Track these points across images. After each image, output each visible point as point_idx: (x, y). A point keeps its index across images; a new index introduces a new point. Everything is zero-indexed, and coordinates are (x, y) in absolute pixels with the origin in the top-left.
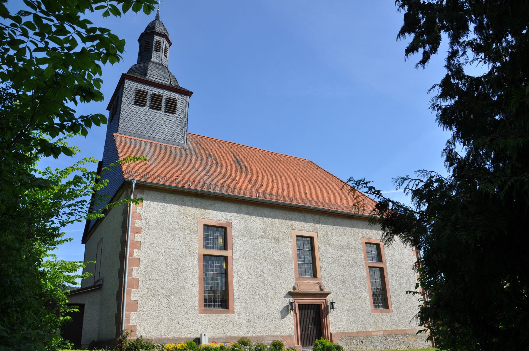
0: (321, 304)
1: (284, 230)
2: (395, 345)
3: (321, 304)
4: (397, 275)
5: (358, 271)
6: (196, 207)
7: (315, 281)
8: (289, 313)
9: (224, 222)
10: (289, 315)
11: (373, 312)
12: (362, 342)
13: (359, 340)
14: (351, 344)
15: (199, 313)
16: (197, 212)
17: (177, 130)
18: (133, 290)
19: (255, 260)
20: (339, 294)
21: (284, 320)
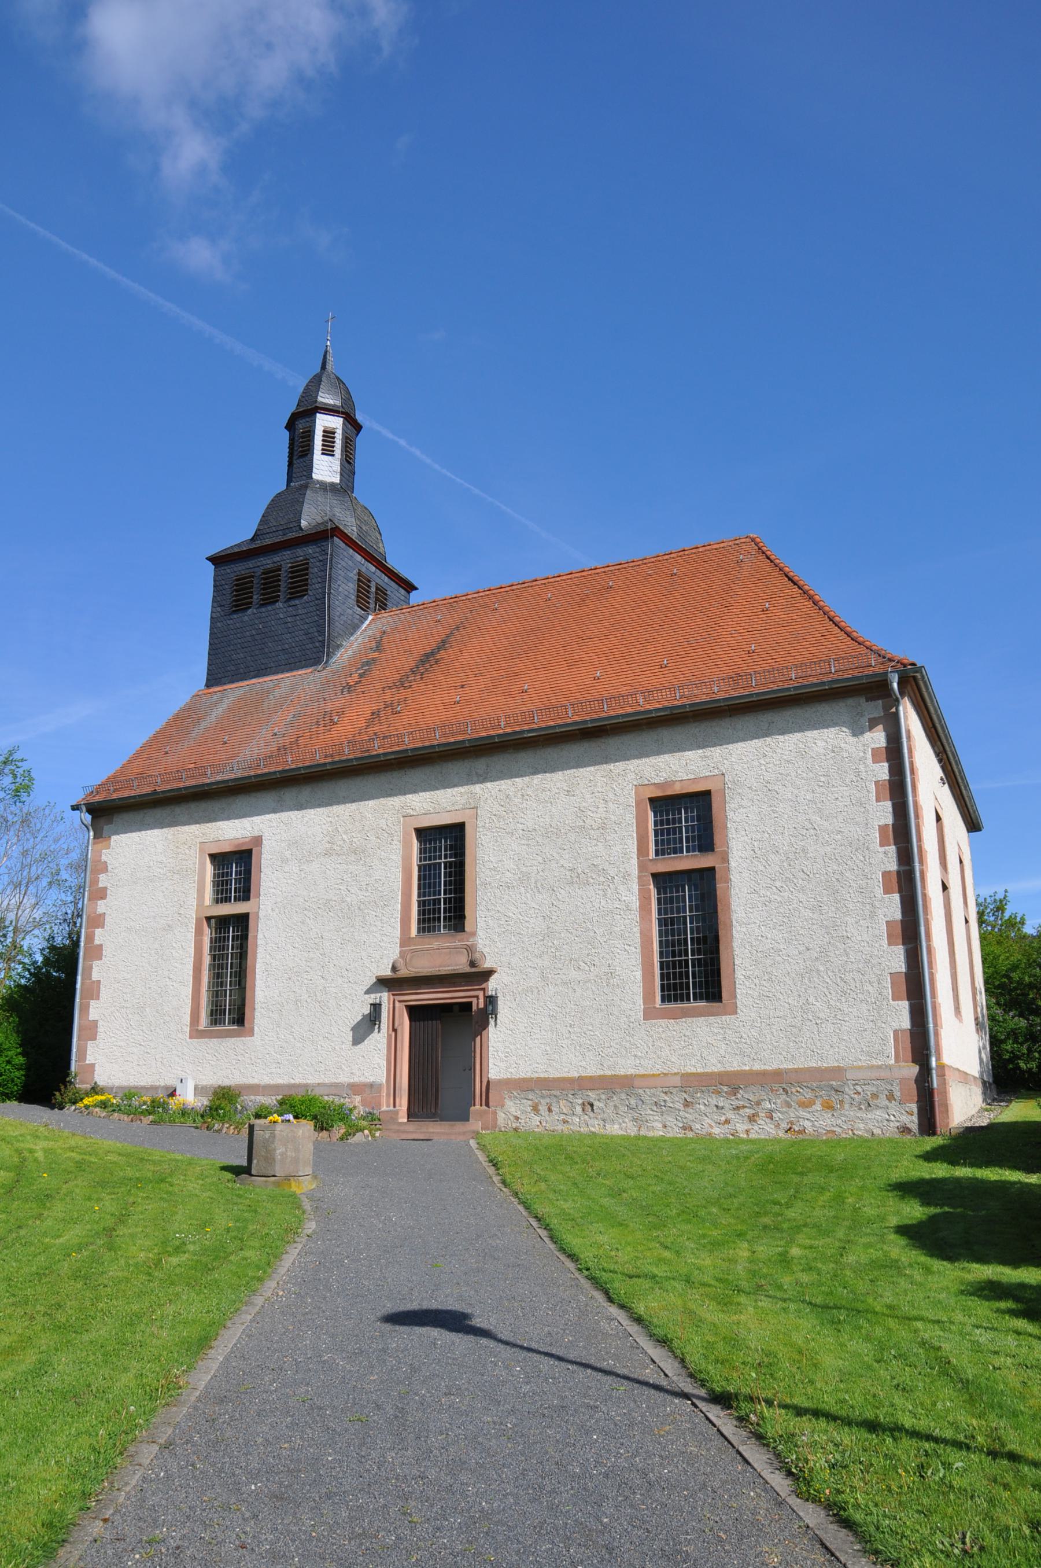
0: (470, 1003)
2: (727, 1122)
3: (470, 1003)
4: (778, 884)
5: (605, 895)
7: (457, 941)
8: (376, 1030)
9: (247, 840)
10: (375, 1035)
11: (649, 1014)
12: (592, 1105)
13: (580, 1101)
14: (550, 1110)
15: (191, 1038)
16: (197, 832)
17: (311, 630)
18: (92, 1003)
19: (306, 912)
20: (529, 970)
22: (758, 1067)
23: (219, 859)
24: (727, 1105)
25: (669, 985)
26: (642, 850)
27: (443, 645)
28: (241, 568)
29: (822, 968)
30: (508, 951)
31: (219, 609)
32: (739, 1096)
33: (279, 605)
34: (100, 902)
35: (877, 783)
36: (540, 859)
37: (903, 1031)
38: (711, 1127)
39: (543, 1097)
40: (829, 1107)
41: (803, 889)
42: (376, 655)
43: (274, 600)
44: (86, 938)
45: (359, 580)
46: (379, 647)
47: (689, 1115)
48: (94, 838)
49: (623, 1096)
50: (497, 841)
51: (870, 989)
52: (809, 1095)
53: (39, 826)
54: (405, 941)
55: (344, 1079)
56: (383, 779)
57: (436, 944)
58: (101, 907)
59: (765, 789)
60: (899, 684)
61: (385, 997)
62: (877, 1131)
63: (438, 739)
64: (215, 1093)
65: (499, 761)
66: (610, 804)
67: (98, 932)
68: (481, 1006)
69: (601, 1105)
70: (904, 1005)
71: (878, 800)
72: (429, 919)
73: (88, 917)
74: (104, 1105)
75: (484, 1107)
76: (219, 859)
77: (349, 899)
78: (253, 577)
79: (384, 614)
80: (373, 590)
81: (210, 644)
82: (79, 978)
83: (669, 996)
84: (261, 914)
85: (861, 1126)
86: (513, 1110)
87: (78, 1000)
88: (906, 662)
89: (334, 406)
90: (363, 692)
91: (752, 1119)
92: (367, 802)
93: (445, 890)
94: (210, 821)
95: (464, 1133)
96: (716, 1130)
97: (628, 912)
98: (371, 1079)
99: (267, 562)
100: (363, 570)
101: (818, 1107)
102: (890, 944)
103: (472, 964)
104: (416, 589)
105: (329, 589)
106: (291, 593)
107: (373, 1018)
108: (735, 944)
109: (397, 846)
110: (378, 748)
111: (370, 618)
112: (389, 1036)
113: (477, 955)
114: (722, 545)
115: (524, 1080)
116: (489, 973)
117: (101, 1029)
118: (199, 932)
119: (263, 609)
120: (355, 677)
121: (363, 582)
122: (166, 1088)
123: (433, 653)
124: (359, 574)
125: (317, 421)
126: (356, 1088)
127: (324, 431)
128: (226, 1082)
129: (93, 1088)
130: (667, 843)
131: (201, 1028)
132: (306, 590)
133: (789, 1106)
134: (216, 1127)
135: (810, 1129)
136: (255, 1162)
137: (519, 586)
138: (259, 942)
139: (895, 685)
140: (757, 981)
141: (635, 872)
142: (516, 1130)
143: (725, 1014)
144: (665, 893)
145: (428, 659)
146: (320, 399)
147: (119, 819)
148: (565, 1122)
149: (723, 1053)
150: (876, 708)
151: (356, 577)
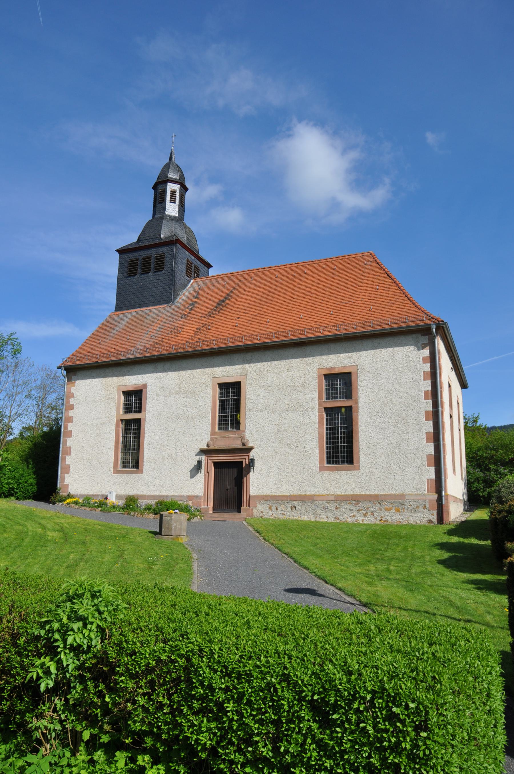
0: (242, 462)
1: (203, 380)
2: (354, 516)
3: (242, 462)
4: (380, 414)
5: (303, 416)
6: (116, 376)
7: (237, 434)
11: (321, 469)
12: (295, 507)
13: (290, 506)
14: (277, 509)
15: (114, 473)
17: (166, 287)
20: (269, 448)
21: (193, 479)
22: (368, 493)
23: (127, 394)
24: (354, 509)
25: (330, 456)
26: (320, 397)
27: (228, 297)
28: (132, 256)
29: (397, 452)
30: (259, 439)
31: (121, 275)
32: (360, 505)
33: (151, 274)
34: (70, 411)
35: (424, 372)
36: (274, 399)
37: (431, 480)
38: (347, 518)
39: (274, 503)
40: (398, 511)
41: (390, 417)
42: (196, 300)
43: (148, 272)
44: (64, 427)
45: (187, 263)
46: (197, 296)
47: (338, 513)
48: (68, 381)
49: (309, 504)
50: (255, 390)
51: (418, 461)
52: (390, 506)
53: (22, 368)
54: (213, 433)
55: (184, 493)
56: (204, 360)
57: (227, 435)
58: (71, 413)
59: (375, 373)
60: (436, 329)
61: (203, 458)
62: (418, 522)
63: (229, 344)
64: (127, 499)
65: (257, 355)
66: (306, 376)
67: (70, 425)
68: (247, 463)
69: (299, 507)
70: (433, 469)
71: (424, 380)
72: (224, 424)
73: (65, 418)
74: (76, 503)
75: (248, 507)
76: (127, 394)
77: (187, 414)
78: (138, 260)
79: (198, 280)
80: (193, 268)
81: (117, 291)
82: (61, 445)
83: (330, 461)
84: (147, 419)
85: (412, 519)
86: (260, 508)
87: (60, 455)
88: (439, 319)
89: (176, 179)
90: (192, 318)
91: (365, 515)
92: (196, 370)
93: (231, 411)
94: (123, 376)
95: (240, 518)
96: (349, 520)
97: (313, 424)
98: (197, 494)
99: (145, 254)
100: (189, 258)
101: (393, 511)
102: (427, 442)
103: (243, 444)
104: (212, 267)
105: (174, 268)
106: (156, 269)
107: (198, 467)
108: (360, 440)
109: (210, 391)
110: (202, 347)
111: (192, 281)
112: (205, 475)
113: (246, 441)
114: (357, 256)
115: (266, 496)
116: (251, 449)
117: (71, 469)
118: (117, 426)
119: (143, 276)
120: (187, 311)
121: (189, 264)
122: (103, 496)
123: (223, 301)
124: (187, 261)
125: (168, 187)
126: (190, 497)
127: (171, 191)
128: (131, 494)
129: (68, 495)
130: (331, 394)
131: (118, 469)
132: (163, 268)
133: (381, 510)
134: (132, 514)
135: (389, 520)
136: (163, 529)
137: (262, 270)
138: (146, 432)
139: (434, 330)
140: (369, 456)
141: (317, 406)
142: (261, 517)
143: (355, 470)
144: (330, 416)
145: (220, 303)
146: (169, 176)
147: (79, 374)
148: (283, 514)
149: (353, 487)
150: (425, 339)
151: (186, 262)
